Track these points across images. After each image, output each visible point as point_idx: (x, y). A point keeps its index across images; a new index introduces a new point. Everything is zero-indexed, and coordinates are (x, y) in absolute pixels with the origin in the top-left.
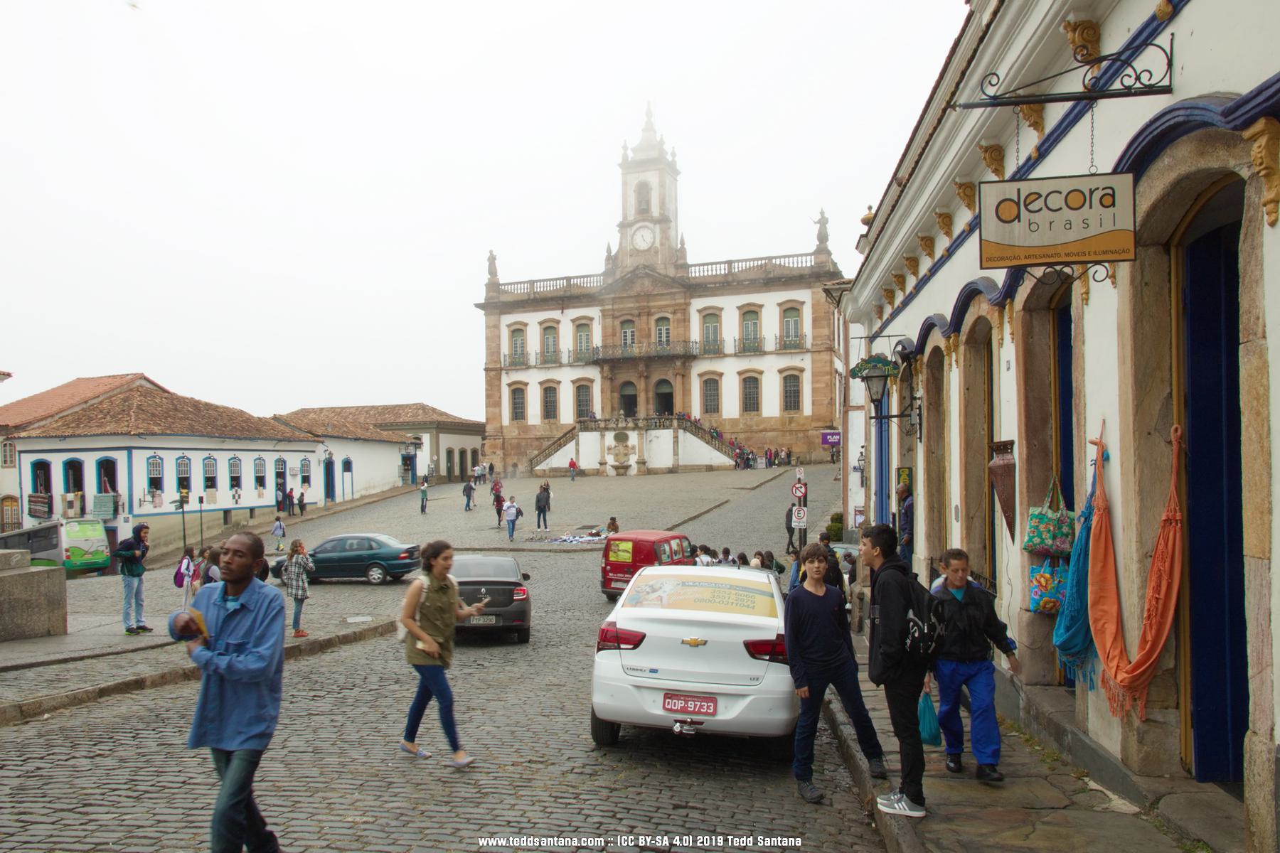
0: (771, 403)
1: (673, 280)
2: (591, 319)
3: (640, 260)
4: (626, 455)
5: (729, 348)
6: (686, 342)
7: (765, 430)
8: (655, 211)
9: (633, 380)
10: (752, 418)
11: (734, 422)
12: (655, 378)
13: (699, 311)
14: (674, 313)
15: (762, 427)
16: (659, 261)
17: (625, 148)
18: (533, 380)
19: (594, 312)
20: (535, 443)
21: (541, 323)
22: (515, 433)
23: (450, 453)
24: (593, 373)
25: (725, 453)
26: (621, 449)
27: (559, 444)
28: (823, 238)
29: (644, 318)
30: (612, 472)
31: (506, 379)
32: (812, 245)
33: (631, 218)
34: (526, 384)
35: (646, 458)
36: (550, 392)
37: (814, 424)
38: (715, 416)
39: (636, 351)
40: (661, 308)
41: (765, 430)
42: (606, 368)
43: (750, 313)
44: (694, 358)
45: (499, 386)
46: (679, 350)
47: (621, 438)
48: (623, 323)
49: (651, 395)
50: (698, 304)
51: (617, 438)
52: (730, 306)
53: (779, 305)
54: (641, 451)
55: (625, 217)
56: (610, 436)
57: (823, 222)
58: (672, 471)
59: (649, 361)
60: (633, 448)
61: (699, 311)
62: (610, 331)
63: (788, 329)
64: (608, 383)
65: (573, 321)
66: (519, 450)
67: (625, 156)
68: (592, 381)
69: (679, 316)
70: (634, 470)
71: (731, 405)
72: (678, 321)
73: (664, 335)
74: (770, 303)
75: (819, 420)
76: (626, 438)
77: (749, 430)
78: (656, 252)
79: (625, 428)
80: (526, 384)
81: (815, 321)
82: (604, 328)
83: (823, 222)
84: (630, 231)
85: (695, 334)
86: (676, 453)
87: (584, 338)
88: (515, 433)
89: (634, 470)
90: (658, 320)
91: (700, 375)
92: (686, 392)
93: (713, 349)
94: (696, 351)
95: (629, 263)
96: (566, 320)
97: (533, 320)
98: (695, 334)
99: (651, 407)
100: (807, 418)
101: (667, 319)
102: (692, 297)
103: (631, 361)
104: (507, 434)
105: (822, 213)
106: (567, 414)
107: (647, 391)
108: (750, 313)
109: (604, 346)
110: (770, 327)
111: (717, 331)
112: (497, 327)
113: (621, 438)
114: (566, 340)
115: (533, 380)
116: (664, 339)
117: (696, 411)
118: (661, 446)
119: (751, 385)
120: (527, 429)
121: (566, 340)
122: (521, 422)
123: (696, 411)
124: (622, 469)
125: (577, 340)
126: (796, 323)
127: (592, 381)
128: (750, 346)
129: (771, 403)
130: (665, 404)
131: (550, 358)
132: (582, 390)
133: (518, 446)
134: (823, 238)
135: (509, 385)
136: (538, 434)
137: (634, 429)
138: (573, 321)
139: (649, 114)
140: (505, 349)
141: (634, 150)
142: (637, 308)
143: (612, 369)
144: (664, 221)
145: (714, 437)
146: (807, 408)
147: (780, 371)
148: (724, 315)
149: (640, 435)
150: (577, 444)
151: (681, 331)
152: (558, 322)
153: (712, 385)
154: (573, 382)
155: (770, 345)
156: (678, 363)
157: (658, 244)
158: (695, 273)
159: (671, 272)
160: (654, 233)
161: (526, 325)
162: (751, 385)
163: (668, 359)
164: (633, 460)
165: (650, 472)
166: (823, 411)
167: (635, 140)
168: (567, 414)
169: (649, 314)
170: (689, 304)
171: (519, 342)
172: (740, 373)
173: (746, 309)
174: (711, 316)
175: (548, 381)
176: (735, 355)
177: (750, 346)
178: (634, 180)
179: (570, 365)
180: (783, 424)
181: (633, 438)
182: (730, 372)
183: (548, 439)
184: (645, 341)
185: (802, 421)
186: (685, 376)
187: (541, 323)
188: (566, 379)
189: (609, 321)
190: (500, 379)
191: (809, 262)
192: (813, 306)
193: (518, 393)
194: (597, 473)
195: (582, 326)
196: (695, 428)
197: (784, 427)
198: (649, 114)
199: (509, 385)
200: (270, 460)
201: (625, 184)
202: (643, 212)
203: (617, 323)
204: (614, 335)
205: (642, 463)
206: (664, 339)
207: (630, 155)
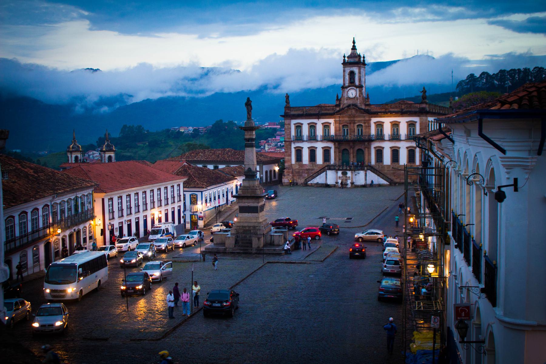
0: (403, 160)
1: (364, 110)
2: (330, 123)
3: (351, 102)
4: (346, 180)
5: (387, 138)
6: (370, 135)
8: (357, 83)
9: (347, 148)
12: (357, 148)
13: (375, 123)
14: (365, 123)
16: (358, 102)
17: (344, 57)
18: (305, 147)
19: (331, 121)
20: (306, 171)
21: (308, 124)
22: (297, 167)
23: (266, 172)
24: (330, 145)
25: (385, 180)
26: (344, 178)
27: (318, 173)
29: (352, 125)
31: (293, 146)
33: (347, 85)
35: (354, 181)
38: (381, 164)
39: (349, 137)
40: (359, 121)
42: (337, 144)
45: (291, 148)
47: (344, 174)
48: (343, 126)
51: (342, 173)
53: (407, 122)
54: (352, 179)
55: (344, 84)
56: (340, 173)
58: (364, 186)
59: (354, 142)
60: (349, 177)
61: (375, 123)
62: (338, 129)
63: (410, 132)
64: (337, 150)
65: (322, 124)
66: (299, 173)
67: (344, 60)
68: (330, 148)
69: (367, 124)
71: (387, 159)
72: (366, 126)
73: (360, 131)
76: (346, 173)
78: (357, 99)
79: (347, 170)
80: (302, 148)
82: (335, 128)
84: (346, 90)
85: (373, 131)
86: (366, 180)
87: (327, 131)
88: (297, 167)
90: (358, 126)
91: (375, 148)
92: (370, 154)
93: (380, 137)
95: (346, 102)
96: (319, 123)
97: (305, 123)
98: (373, 131)
101: (362, 125)
102: (372, 117)
103: (348, 142)
104: (294, 168)
105: (424, 88)
106: (320, 160)
107: (353, 153)
109: (336, 135)
111: (382, 131)
112: (290, 124)
113: (344, 174)
114: (320, 132)
115: (305, 147)
116: (360, 134)
117: (373, 162)
118: (360, 178)
119: (395, 153)
121: (320, 132)
123: (373, 162)
125: (324, 131)
126: (414, 129)
127: (330, 148)
129: (403, 160)
132: (326, 151)
133: (299, 172)
135: (295, 148)
137: (349, 170)
138: (322, 124)
139: (354, 42)
140: (293, 133)
141: (348, 57)
142: (350, 120)
143: (339, 144)
144: (360, 87)
146: (418, 162)
147: (407, 148)
148: (385, 125)
149: (352, 173)
150: (326, 174)
151: (367, 130)
152: (316, 124)
153: (380, 152)
154: (322, 148)
155: (403, 137)
156: (366, 143)
160: (356, 91)
161: (302, 124)
162: (395, 153)
164: (349, 182)
165: (357, 186)
167: (349, 52)
168: (320, 160)
169: (354, 123)
170: (370, 120)
171: (299, 131)
172: (391, 148)
173: (394, 123)
175: (312, 147)
176: (389, 140)
178: (348, 70)
179: (321, 141)
181: (349, 174)
182: (387, 147)
183: (312, 170)
184: (353, 134)
186: (369, 148)
187: (308, 124)
188: (320, 146)
189: (338, 125)
190: (291, 146)
192: (420, 124)
193: (299, 151)
194: (334, 186)
195: (326, 126)
198: (354, 42)
199: (295, 148)
201: (344, 71)
202: (352, 82)
203: (341, 126)
204: (340, 130)
205: (352, 183)
206: (360, 133)
207: (346, 59)
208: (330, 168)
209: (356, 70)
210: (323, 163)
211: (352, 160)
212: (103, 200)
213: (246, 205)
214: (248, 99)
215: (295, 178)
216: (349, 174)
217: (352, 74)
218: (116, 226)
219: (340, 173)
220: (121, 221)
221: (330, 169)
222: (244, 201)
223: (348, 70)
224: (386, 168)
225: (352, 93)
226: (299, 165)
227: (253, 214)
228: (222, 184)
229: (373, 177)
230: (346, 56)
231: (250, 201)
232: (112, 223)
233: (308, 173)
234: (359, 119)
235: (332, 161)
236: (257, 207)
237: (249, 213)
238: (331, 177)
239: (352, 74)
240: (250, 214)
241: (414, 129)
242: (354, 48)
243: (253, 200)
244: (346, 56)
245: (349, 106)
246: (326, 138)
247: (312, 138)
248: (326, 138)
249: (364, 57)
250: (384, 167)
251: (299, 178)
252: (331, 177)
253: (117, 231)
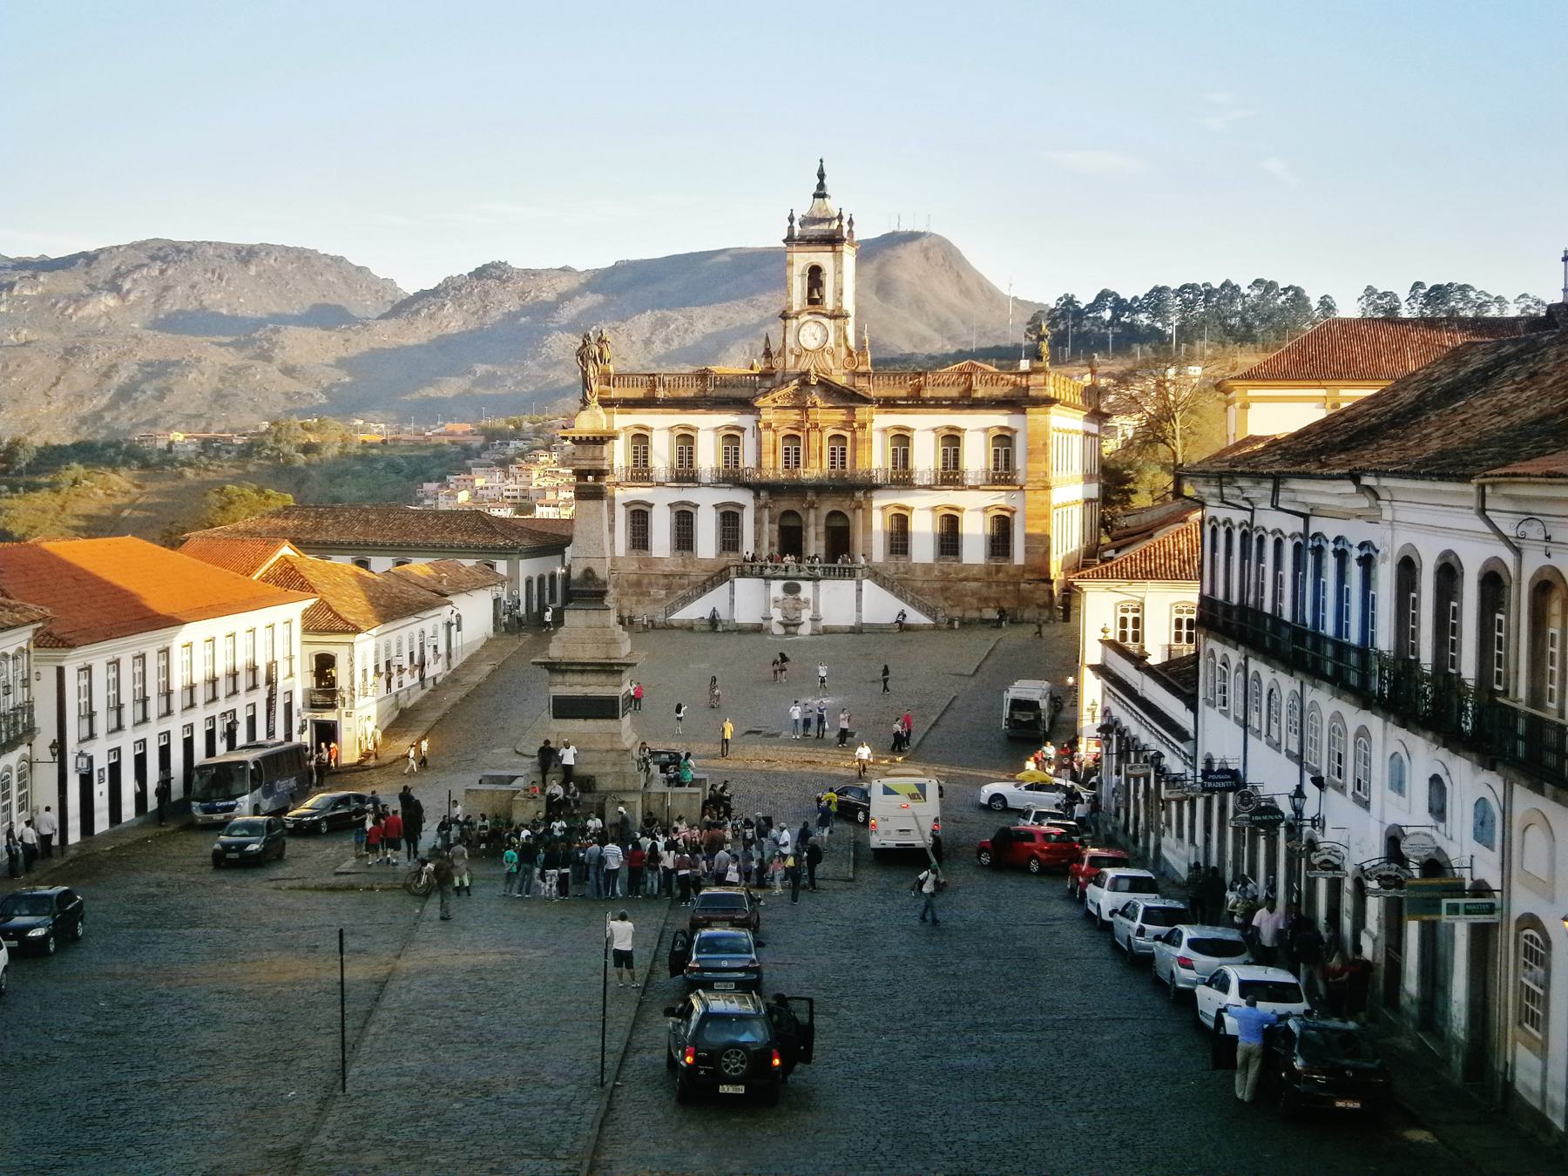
0: (974, 551)
7: (966, 579)
8: (829, 304)
11: (927, 568)
15: (961, 576)
17: (791, 219)
20: (666, 581)
23: (529, 582)
24: (744, 498)
30: (779, 630)
34: (651, 506)
36: (684, 520)
37: (1027, 576)
38: (902, 560)
41: (966, 579)
43: (952, 440)
44: (877, 487)
47: (792, 589)
49: (822, 529)
51: (787, 589)
52: (925, 427)
54: (816, 605)
56: (777, 587)
58: (858, 630)
59: (820, 488)
60: (807, 602)
67: (791, 228)
68: (742, 507)
70: (805, 630)
71: (923, 550)
75: (1032, 571)
76: (797, 589)
77: (945, 577)
81: (1030, 453)
86: (859, 610)
89: (805, 630)
93: (902, 479)
99: (822, 543)
100: (1019, 567)
101: (844, 438)
103: (797, 489)
108: (952, 440)
110: (976, 457)
113: (792, 589)
114: (708, 458)
115: (661, 503)
120: (650, 562)
122: (643, 554)
123: (879, 553)
124: (791, 625)
128: (950, 476)
129: (974, 551)
130: (840, 541)
131: (685, 474)
132: (729, 519)
133: (638, 584)
136: (667, 570)
139: (821, 175)
150: (732, 592)
157: (831, 342)
164: (806, 615)
165: (827, 631)
166: (1038, 561)
175: (682, 503)
177: (950, 476)
180: (989, 574)
181: (807, 588)
183: (682, 576)
185: (1012, 572)
188: (707, 504)
196: (875, 575)
197: (988, 575)
198: (821, 175)
207: (797, 229)
210: (719, 555)
211: (815, 544)
212: (61, 672)
215: (625, 602)
216: (807, 588)
217: (815, 273)
218: (101, 763)
219: (777, 587)
221: (742, 575)
222: (569, 678)
223: (802, 260)
224: (919, 573)
226: (639, 561)
227: (601, 723)
228: (412, 619)
229: (880, 606)
230: (798, 217)
231: (592, 679)
233: (668, 587)
236: (613, 701)
237: (586, 718)
238: (748, 601)
239: (815, 273)
240: (590, 722)
241: (1007, 453)
242: (820, 194)
243: (603, 678)
244: (798, 217)
246: (731, 477)
247: (685, 474)
248: (731, 477)
249: (851, 222)
250: (910, 570)
251: (638, 602)
252: (748, 601)
253: (101, 780)
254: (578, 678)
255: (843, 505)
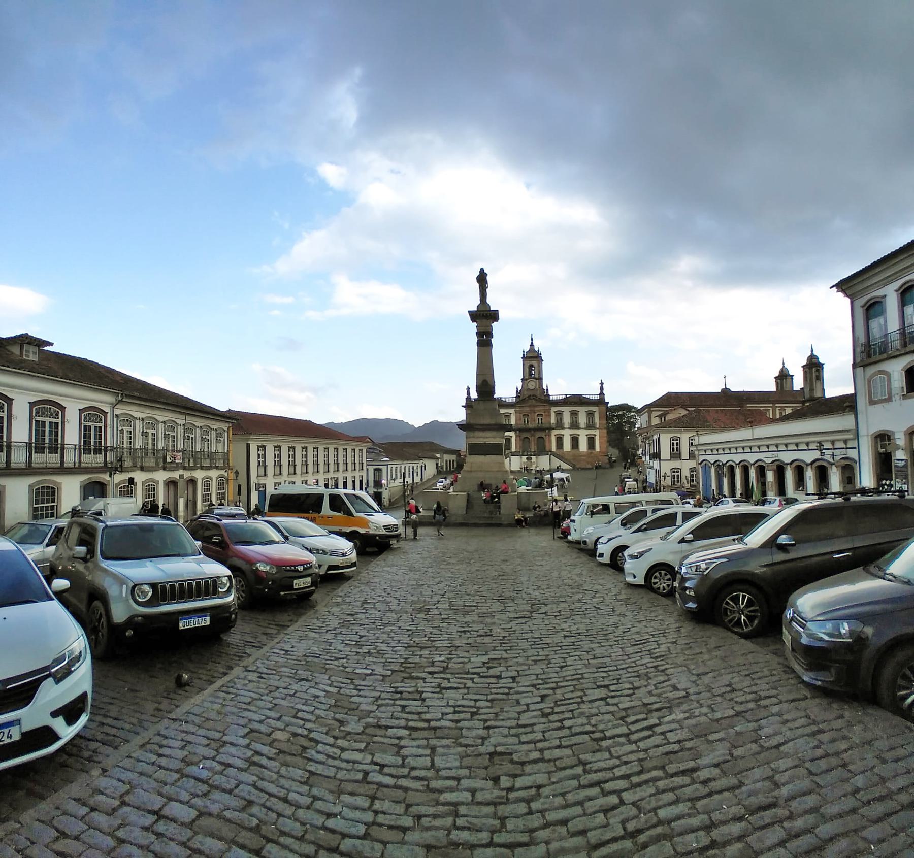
0: (583, 446)
10: (575, 451)
12: (537, 436)
19: (512, 411)
28: (602, 389)
32: (598, 392)
39: (530, 426)
43: (574, 414)
46: (548, 426)
47: (529, 459)
50: (554, 409)
52: (566, 411)
56: (524, 458)
57: (602, 384)
74: (582, 412)
83: (602, 384)
85: (553, 420)
92: (550, 441)
93: (560, 425)
94: (554, 426)
95: (526, 394)
108: (574, 414)
113: (529, 459)
117: (554, 449)
118: (543, 462)
119: (575, 441)
123: (554, 449)
129: (583, 446)
134: (602, 389)
145: (560, 458)
146: (598, 449)
153: (560, 439)
155: (583, 425)
158: (551, 398)
159: (543, 398)
162: (575, 441)
163: (543, 430)
166: (604, 450)
167: (527, 349)
174: (559, 414)
177: (574, 425)
178: (528, 363)
182: (567, 434)
186: (550, 435)
191: (598, 397)
196: (553, 454)
197: (589, 455)
200: (394, 466)
208: (514, 454)
209: (534, 363)
211: (533, 448)
212: (248, 445)
213: (481, 441)
214: (482, 270)
219: (524, 458)
220: (278, 481)
222: (477, 434)
223: (528, 363)
225: (532, 385)
232: (262, 482)
234: (540, 409)
235: (513, 449)
237: (485, 455)
240: (488, 457)
242: (532, 345)
245: (529, 397)
250: (563, 453)
254: (481, 434)
255: (542, 434)
